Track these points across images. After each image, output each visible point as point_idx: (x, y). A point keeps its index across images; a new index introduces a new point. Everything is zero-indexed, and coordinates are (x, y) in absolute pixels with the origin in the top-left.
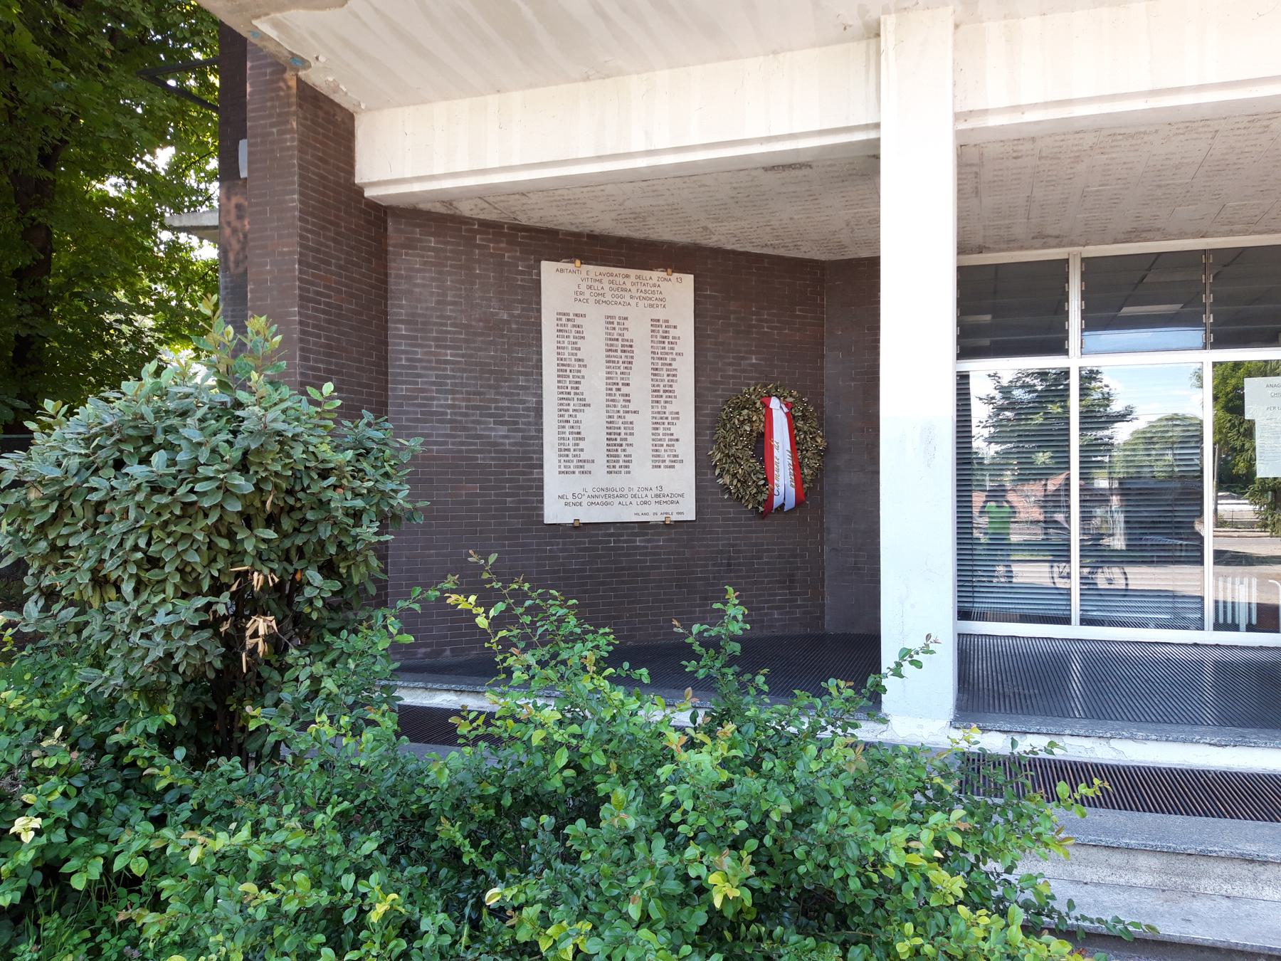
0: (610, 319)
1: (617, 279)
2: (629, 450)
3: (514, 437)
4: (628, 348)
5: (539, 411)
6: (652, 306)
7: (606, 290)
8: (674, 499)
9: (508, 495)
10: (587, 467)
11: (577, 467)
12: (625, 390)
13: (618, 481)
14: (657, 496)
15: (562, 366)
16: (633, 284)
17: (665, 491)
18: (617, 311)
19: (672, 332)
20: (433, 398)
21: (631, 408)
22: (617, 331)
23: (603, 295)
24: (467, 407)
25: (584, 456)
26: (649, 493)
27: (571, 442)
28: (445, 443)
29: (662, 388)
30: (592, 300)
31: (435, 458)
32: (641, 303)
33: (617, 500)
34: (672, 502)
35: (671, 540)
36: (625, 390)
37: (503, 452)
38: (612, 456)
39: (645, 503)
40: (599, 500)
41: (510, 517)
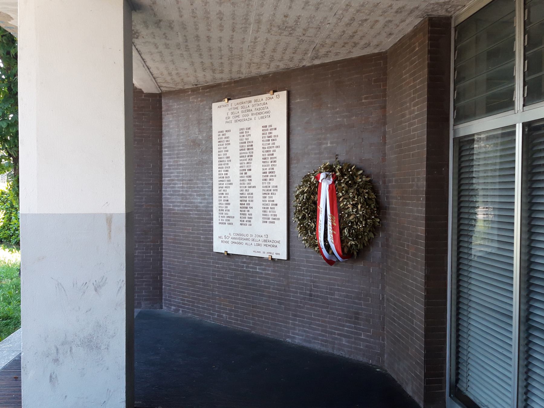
4: (251, 147)
5: (212, 187)
6: (262, 118)
8: (274, 244)
9: (202, 234)
10: (232, 220)
11: (226, 220)
12: (249, 173)
13: (245, 230)
14: (265, 241)
16: (253, 106)
17: (270, 238)
18: (245, 125)
19: (274, 133)
20: (176, 184)
21: (252, 185)
22: (245, 137)
23: (238, 116)
24: (187, 188)
25: (230, 214)
26: (261, 239)
27: (224, 206)
28: (179, 206)
29: (268, 171)
31: (177, 214)
33: (245, 242)
36: (249, 173)
38: (243, 214)
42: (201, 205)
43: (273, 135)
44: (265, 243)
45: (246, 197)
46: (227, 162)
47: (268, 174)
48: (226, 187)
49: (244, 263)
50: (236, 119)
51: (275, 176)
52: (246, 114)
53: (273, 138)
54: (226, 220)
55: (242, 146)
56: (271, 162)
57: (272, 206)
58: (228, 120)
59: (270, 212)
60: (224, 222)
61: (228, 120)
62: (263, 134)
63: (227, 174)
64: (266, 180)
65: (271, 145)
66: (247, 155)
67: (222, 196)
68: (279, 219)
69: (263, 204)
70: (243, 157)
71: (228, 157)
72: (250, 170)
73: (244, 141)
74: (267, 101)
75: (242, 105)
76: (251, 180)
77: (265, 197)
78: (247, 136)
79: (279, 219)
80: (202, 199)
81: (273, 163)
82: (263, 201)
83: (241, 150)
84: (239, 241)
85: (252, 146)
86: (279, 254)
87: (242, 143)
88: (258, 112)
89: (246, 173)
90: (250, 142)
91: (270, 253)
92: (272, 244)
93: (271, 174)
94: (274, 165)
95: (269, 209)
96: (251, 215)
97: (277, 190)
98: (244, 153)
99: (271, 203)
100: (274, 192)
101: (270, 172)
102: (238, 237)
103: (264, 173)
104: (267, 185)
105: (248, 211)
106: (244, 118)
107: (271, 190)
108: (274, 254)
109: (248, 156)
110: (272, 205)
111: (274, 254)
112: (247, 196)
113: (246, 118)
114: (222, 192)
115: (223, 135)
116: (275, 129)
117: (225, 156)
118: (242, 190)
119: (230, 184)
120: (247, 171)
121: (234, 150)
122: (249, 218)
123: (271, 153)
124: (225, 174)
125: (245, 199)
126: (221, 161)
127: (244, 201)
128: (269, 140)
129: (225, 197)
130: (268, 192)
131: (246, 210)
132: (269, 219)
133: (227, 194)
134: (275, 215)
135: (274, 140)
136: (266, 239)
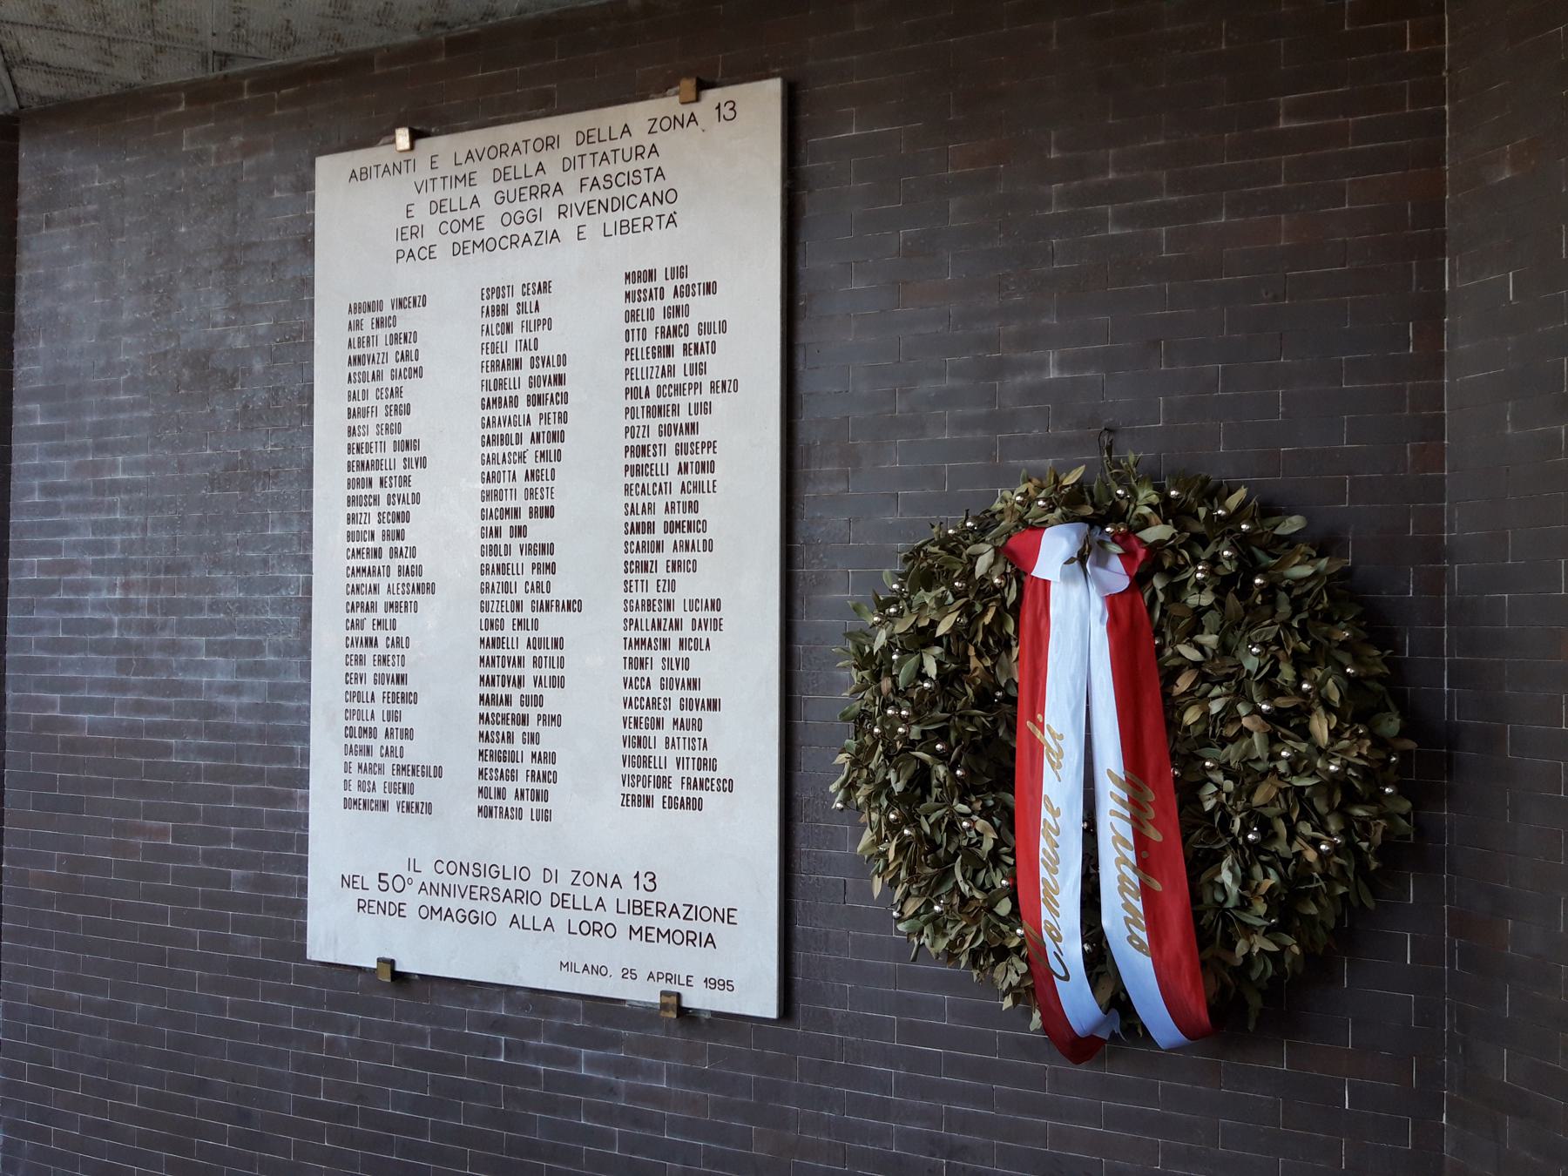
0: (495, 302)
1: (517, 160)
2: (550, 739)
3: (253, 690)
4: (552, 385)
6: (626, 227)
7: (487, 200)
8: (699, 925)
10: (424, 789)
11: (393, 788)
12: (539, 531)
13: (512, 843)
15: (361, 465)
16: (568, 164)
17: (666, 894)
19: (701, 309)
20: (84, 587)
21: (559, 592)
22: (518, 334)
23: (476, 223)
24: (152, 608)
25: (414, 753)
27: (380, 707)
28: (104, 707)
29: (659, 518)
30: (444, 246)
31: (88, 746)
32: (593, 224)
33: (506, 910)
34: (690, 939)
35: (701, 1080)
36: (539, 531)
37: (224, 732)
38: (495, 757)
39: (596, 929)
40: (454, 903)
41: (239, 925)
42: (233, 701)
43: (693, 321)
44: (640, 921)
45: (520, 662)
46: (400, 471)
47: (659, 535)
48: (391, 606)
49: (499, 1025)
50: (460, 237)
51: (708, 546)
52: (525, 207)
53: (694, 337)
54: (393, 788)
55: (499, 384)
56: (683, 469)
57: (687, 715)
58: (414, 244)
59: (670, 743)
60: (379, 795)
61: (414, 244)
62: (632, 316)
63: (399, 535)
64: (644, 567)
65: (679, 378)
66: (526, 431)
67: (369, 653)
68: (728, 785)
69: (628, 703)
70: (504, 440)
71: (408, 445)
72: (548, 512)
73: (512, 354)
74: (658, 139)
75: (500, 163)
76: (551, 568)
77: (642, 663)
78: (527, 326)
79: (728, 785)
80: (240, 670)
81: (692, 477)
82: (628, 683)
83: (487, 404)
84: (467, 905)
85: (559, 379)
86: (727, 985)
87: (496, 366)
88: (602, 195)
89: (520, 531)
90: (547, 362)
91: (669, 978)
92: (685, 926)
93: (679, 536)
94: (698, 487)
95: (668, 730)
96: (551, 758)
97: (717, 625)
98: (509, 421)
99: (676, 695)
100: (702, 634)
101: (672, 527)
102: (463, 881)
103: (636, 528)
104: (652, 594)
105: (533, 738)
106: (513, 229)
107: (676, 625)
108: (698, 982)
109: (536, 438)
110: (687, 704)
111: (698, 982)
112: (529, 655)
113: (522, 230)
114: (368, 632)
115: (379, 323)
116: (710, 288)
117: (389, 439)
118: (491, 625)
119: (419, 589)
120: (524, 519)
121: (446, 407)
122: (534, 776)
123: (684, 418)
124: (386, 535)
125: (514, 672)
126: (363, 466)
127: (506, 681)
128: (669, 351)
129: (384, 660)
130: (659, 632)
131: (518, 731)
132: (663, 782)
133: (397, 643)
134: (703, 764)
135: (698, 349)
136: (643, 896)
